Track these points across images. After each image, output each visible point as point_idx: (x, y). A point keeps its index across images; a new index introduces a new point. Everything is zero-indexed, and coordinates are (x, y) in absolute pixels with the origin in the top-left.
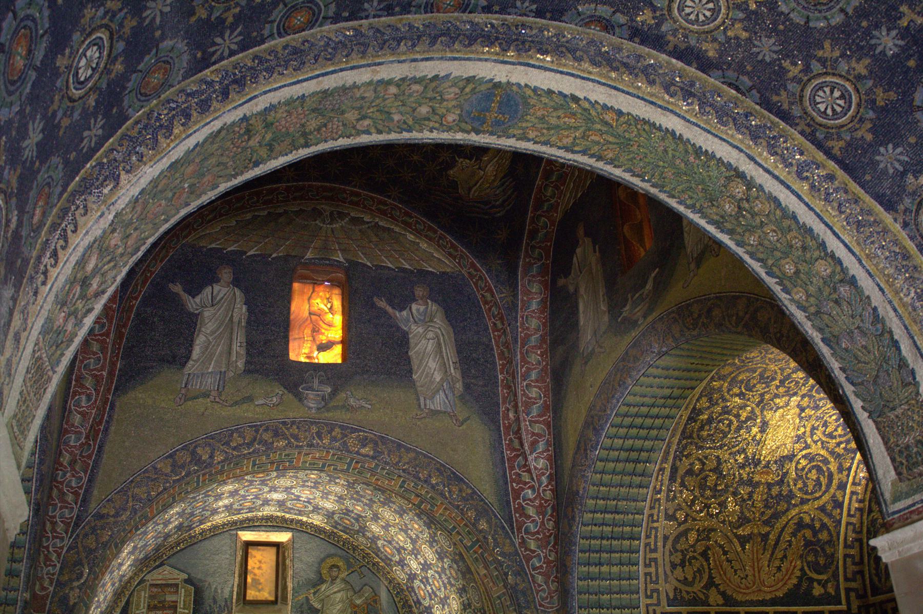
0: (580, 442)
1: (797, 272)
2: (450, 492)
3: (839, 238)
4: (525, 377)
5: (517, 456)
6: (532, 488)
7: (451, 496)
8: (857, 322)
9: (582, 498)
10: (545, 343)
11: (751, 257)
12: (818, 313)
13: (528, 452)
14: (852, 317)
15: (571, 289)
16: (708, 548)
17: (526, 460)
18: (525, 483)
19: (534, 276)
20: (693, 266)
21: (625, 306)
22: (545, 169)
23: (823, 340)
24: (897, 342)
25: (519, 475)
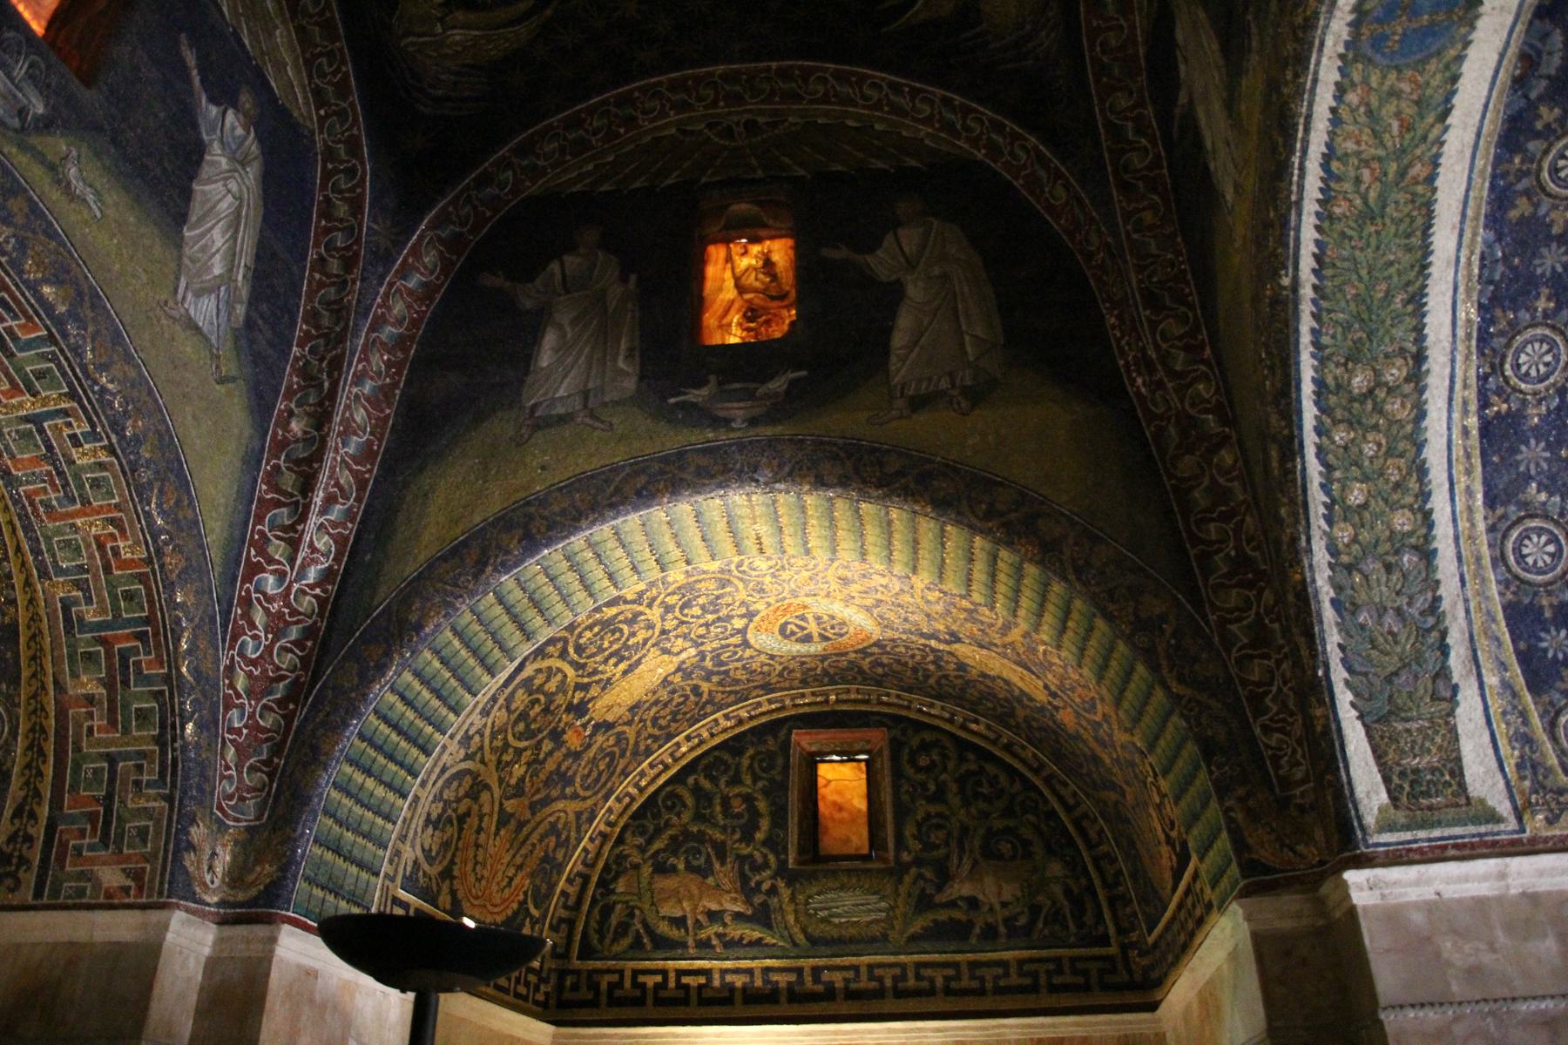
0: (464, 544)
1: (1365, 506)
2: (161, 491)
3: (1452, 499)
4: (359, 379)
5: (279, 504)
6: (281, 575)
7: (159, 505)
8: (1403, 601)
10: (405, 350)
11: (1318, 455)
12: (1349, 568)
14: (1398, 593)
16: (468, 814)
17: (303, 518)
18: (271, 561)
20: (900, 403)
21: (698, 386)
22: (579, 111)
23: (1333, 601)
24: (1447, 646)
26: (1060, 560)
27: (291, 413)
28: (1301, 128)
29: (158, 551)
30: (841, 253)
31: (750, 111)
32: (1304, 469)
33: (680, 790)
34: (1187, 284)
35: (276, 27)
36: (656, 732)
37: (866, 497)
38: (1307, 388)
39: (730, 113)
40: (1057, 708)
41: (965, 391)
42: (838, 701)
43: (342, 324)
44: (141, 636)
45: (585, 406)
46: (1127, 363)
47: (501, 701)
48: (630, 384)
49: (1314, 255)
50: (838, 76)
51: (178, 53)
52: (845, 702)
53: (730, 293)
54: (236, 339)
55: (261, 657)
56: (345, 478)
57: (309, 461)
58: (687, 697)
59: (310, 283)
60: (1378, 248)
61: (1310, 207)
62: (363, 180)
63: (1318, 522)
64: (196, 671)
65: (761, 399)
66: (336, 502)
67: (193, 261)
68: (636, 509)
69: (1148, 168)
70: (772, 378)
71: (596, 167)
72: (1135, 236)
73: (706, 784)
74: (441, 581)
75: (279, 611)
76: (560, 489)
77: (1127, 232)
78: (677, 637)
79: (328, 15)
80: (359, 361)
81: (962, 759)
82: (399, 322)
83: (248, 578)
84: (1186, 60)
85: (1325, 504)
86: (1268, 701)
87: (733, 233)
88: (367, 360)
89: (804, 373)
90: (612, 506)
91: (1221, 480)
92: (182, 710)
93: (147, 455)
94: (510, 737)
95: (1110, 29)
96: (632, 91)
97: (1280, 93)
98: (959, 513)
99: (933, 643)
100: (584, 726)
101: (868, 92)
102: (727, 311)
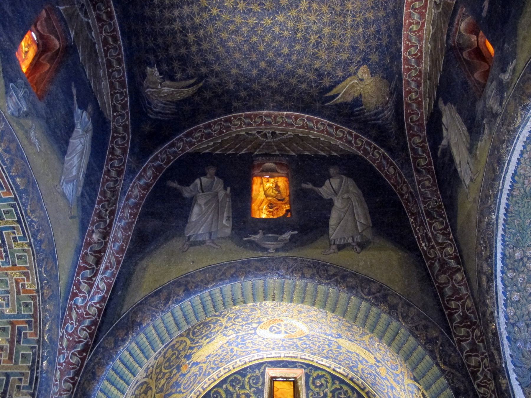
0: (160, 291)
1: (519, 301)
4: (120, 221)
5: (86, 268)
6: (84, 298)
9: (141, 330)
11: (502, 281)
12: (513, 325)
13: (101, 271)
15: (187, 195)
17: (95, 275)
18: (81, 292)
19: (153, 165)
20: (334, 247)
21: (256, 233)
25: (80, 283)
26: (397, 313)
27: (93, 232)
28: (506, 164)
29: (42, 288)
30: (309, 186)
31: (274, 128)
32: (496, 286)
33: (220, 390)
34: (443, 210)
35: (102, 81)
36: (214, 366)
37: (320, 283)
38: (499, 256)
39: (266, 129)
40: (378, 367)
41: (359, 244)
42: (284, 357)
43: (115, 197)
44: (29, 322)
45: (210, 238)
46: (418, 238)
47: (162, 354)
48: (228, 231)
49: (505, 208)
50: (308, 119)
51: (71, 89)
52: (288, 357)
53: (262, 196)
54: (78, 201)
55: (73, 332)
56: (113, 260)
57: (99, 252)
58: (228, 353)
59: (103, 179)
60: (528, 207)
61: (506, 191)
62: (128, 141)
63: (501, 307)
64: (50, 339)
65: (280, 241)
66: (109, 269)
67: (67, 170)
68: (230, 281)
69: (426, 165)
70: (284, 233)
71: (214, 143)
72: (422, 190)
73: (231, 389)
74: (150, 305)
75: (82, 313)
76: (200, 271)
77: (419, 188)
78: (230, 330)
79: (123, 79)
80: (121, 212)
81: (334, 383)
82: (136, 198)
83: (72, 299)
84: (447, 130)
85: (504, 300)
86: (478, 374)
87: (264, 173)
88: (124, 212)
89: (297, 232)
90: (221, 280)
91: (456, 285)
92: (43, 356)
93: (44, 248)
94: (163, 368)
95: (413, 114)
96: (231, 117)
97: (499, 152)
98: (357, 292)
99: (330, 338)
100: (189, 364)
101: (319, 126)
102: (261, 203)
